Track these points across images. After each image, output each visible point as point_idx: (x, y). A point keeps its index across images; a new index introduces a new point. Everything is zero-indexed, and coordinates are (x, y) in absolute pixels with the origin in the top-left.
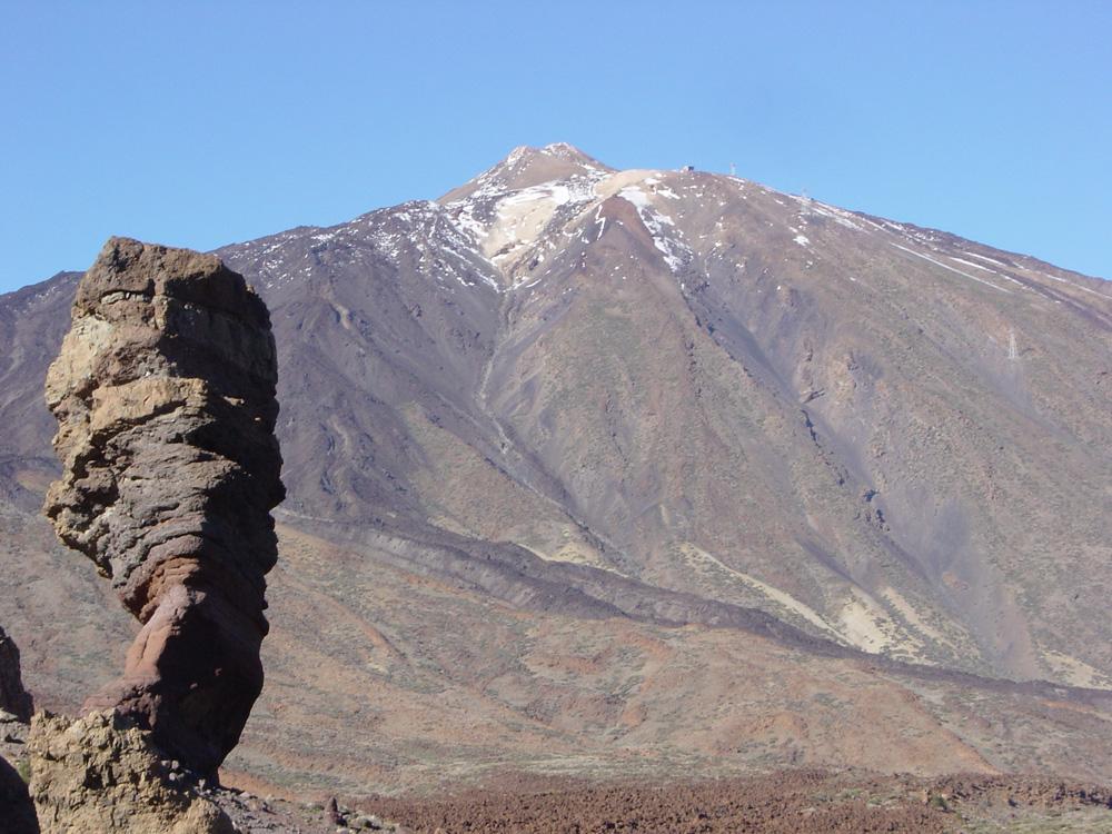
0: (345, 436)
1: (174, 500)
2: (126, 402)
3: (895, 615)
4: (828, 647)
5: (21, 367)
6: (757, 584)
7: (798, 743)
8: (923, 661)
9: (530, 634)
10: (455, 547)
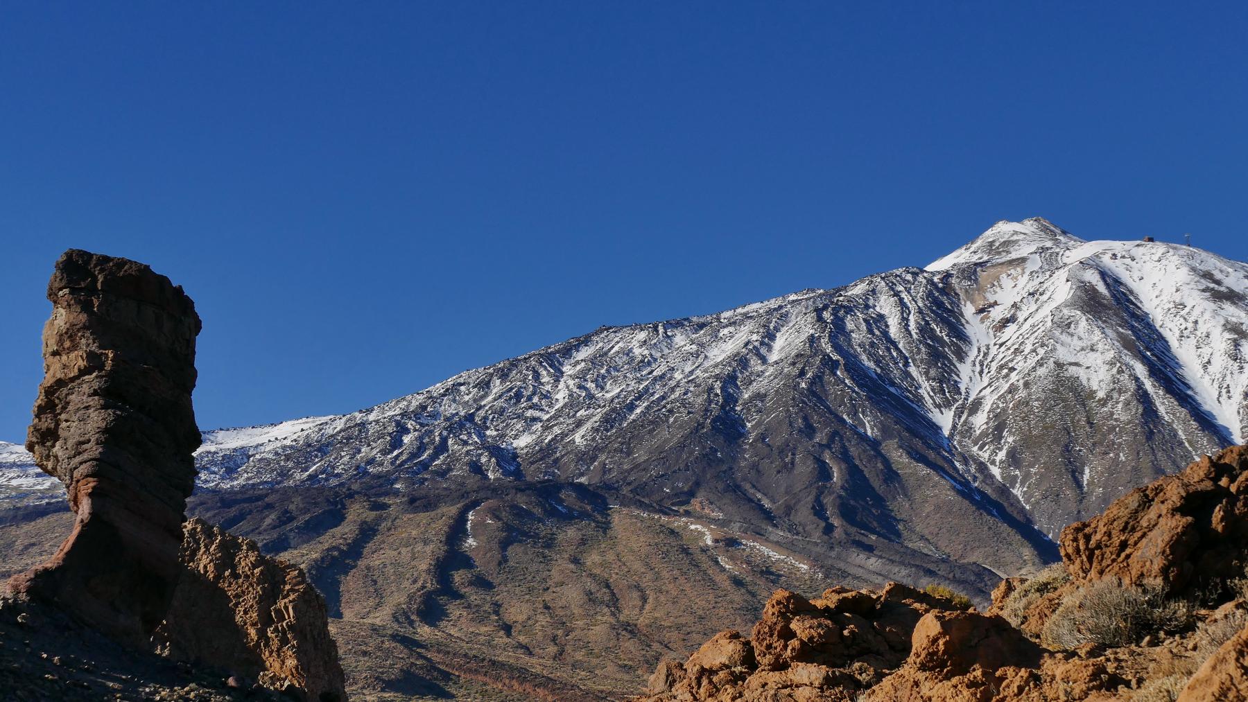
0: (835, 470)
1: (87, 437)
2: (65, 367)
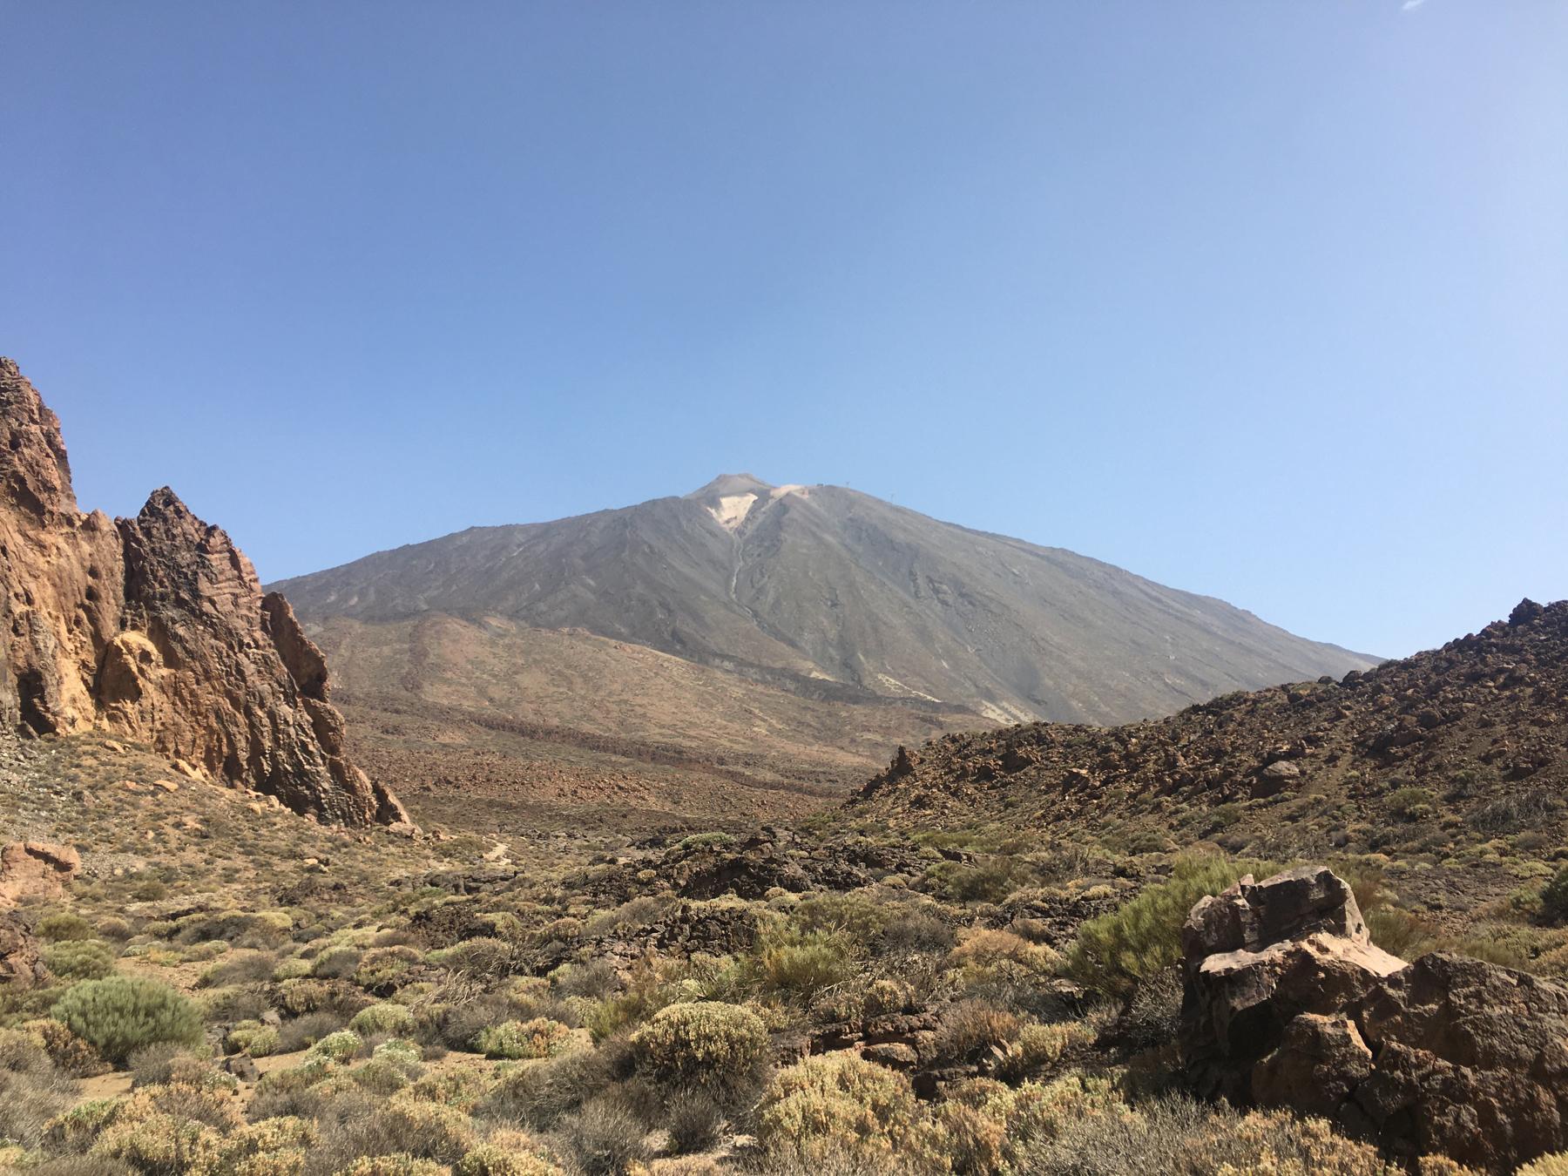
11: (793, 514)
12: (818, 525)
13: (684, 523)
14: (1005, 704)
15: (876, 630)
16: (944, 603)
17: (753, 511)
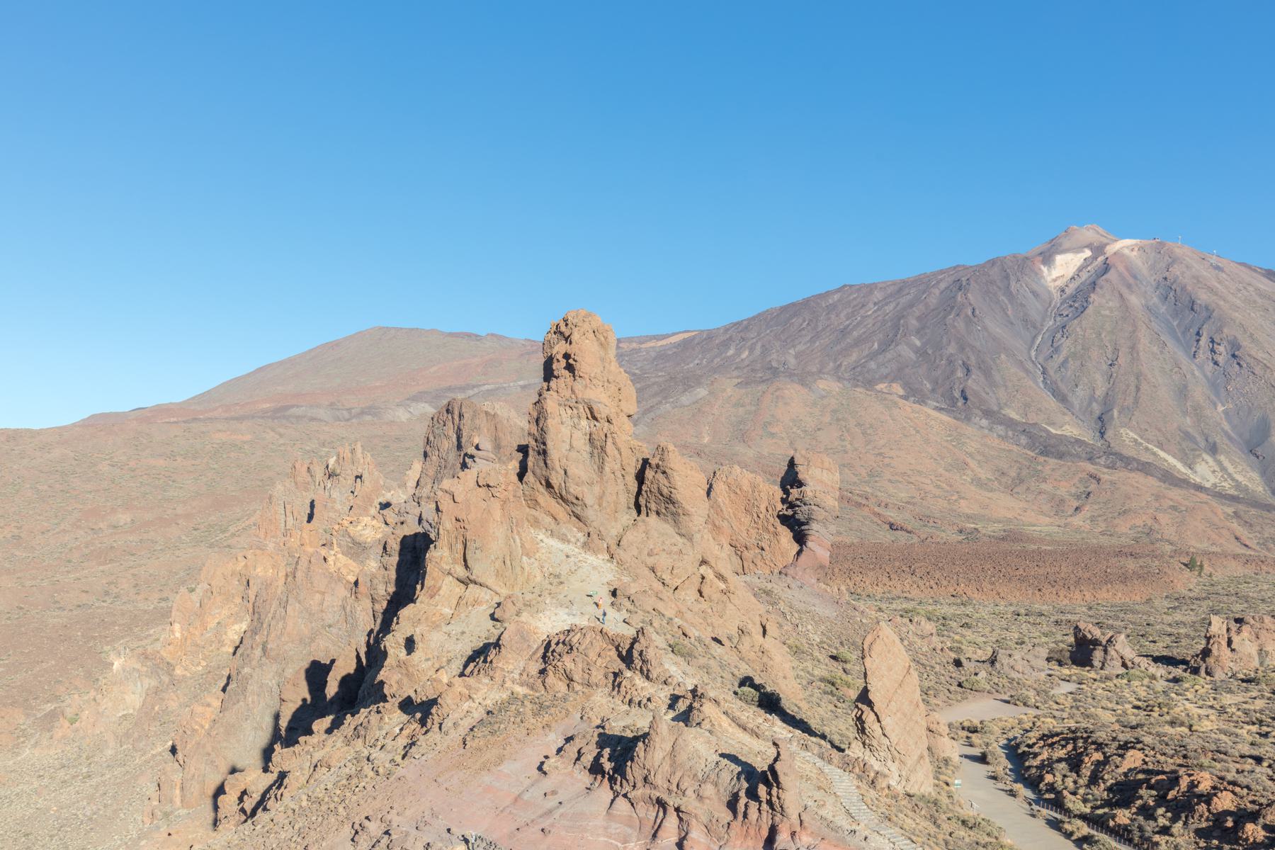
3: (1223, 469)
4: (1183, 483)
5: (824, 329)
6: (1155, 449)
7: (1156, 527)
8: (1232, 492)
9: (1039, 468)
10: (1010, 423)
11: (1111, 275)
12: (1129, 286)
13: (1013, 284)
14: (1222, 458)
15: (1138, 389)
16: (1216, 363)
17: (1080, 270)
